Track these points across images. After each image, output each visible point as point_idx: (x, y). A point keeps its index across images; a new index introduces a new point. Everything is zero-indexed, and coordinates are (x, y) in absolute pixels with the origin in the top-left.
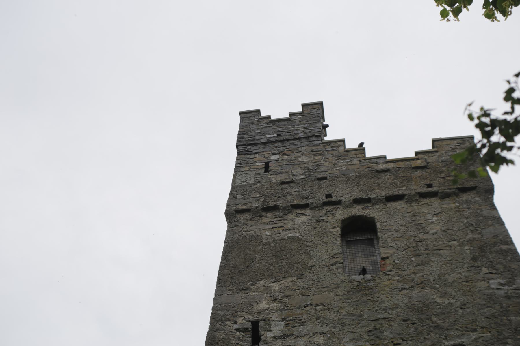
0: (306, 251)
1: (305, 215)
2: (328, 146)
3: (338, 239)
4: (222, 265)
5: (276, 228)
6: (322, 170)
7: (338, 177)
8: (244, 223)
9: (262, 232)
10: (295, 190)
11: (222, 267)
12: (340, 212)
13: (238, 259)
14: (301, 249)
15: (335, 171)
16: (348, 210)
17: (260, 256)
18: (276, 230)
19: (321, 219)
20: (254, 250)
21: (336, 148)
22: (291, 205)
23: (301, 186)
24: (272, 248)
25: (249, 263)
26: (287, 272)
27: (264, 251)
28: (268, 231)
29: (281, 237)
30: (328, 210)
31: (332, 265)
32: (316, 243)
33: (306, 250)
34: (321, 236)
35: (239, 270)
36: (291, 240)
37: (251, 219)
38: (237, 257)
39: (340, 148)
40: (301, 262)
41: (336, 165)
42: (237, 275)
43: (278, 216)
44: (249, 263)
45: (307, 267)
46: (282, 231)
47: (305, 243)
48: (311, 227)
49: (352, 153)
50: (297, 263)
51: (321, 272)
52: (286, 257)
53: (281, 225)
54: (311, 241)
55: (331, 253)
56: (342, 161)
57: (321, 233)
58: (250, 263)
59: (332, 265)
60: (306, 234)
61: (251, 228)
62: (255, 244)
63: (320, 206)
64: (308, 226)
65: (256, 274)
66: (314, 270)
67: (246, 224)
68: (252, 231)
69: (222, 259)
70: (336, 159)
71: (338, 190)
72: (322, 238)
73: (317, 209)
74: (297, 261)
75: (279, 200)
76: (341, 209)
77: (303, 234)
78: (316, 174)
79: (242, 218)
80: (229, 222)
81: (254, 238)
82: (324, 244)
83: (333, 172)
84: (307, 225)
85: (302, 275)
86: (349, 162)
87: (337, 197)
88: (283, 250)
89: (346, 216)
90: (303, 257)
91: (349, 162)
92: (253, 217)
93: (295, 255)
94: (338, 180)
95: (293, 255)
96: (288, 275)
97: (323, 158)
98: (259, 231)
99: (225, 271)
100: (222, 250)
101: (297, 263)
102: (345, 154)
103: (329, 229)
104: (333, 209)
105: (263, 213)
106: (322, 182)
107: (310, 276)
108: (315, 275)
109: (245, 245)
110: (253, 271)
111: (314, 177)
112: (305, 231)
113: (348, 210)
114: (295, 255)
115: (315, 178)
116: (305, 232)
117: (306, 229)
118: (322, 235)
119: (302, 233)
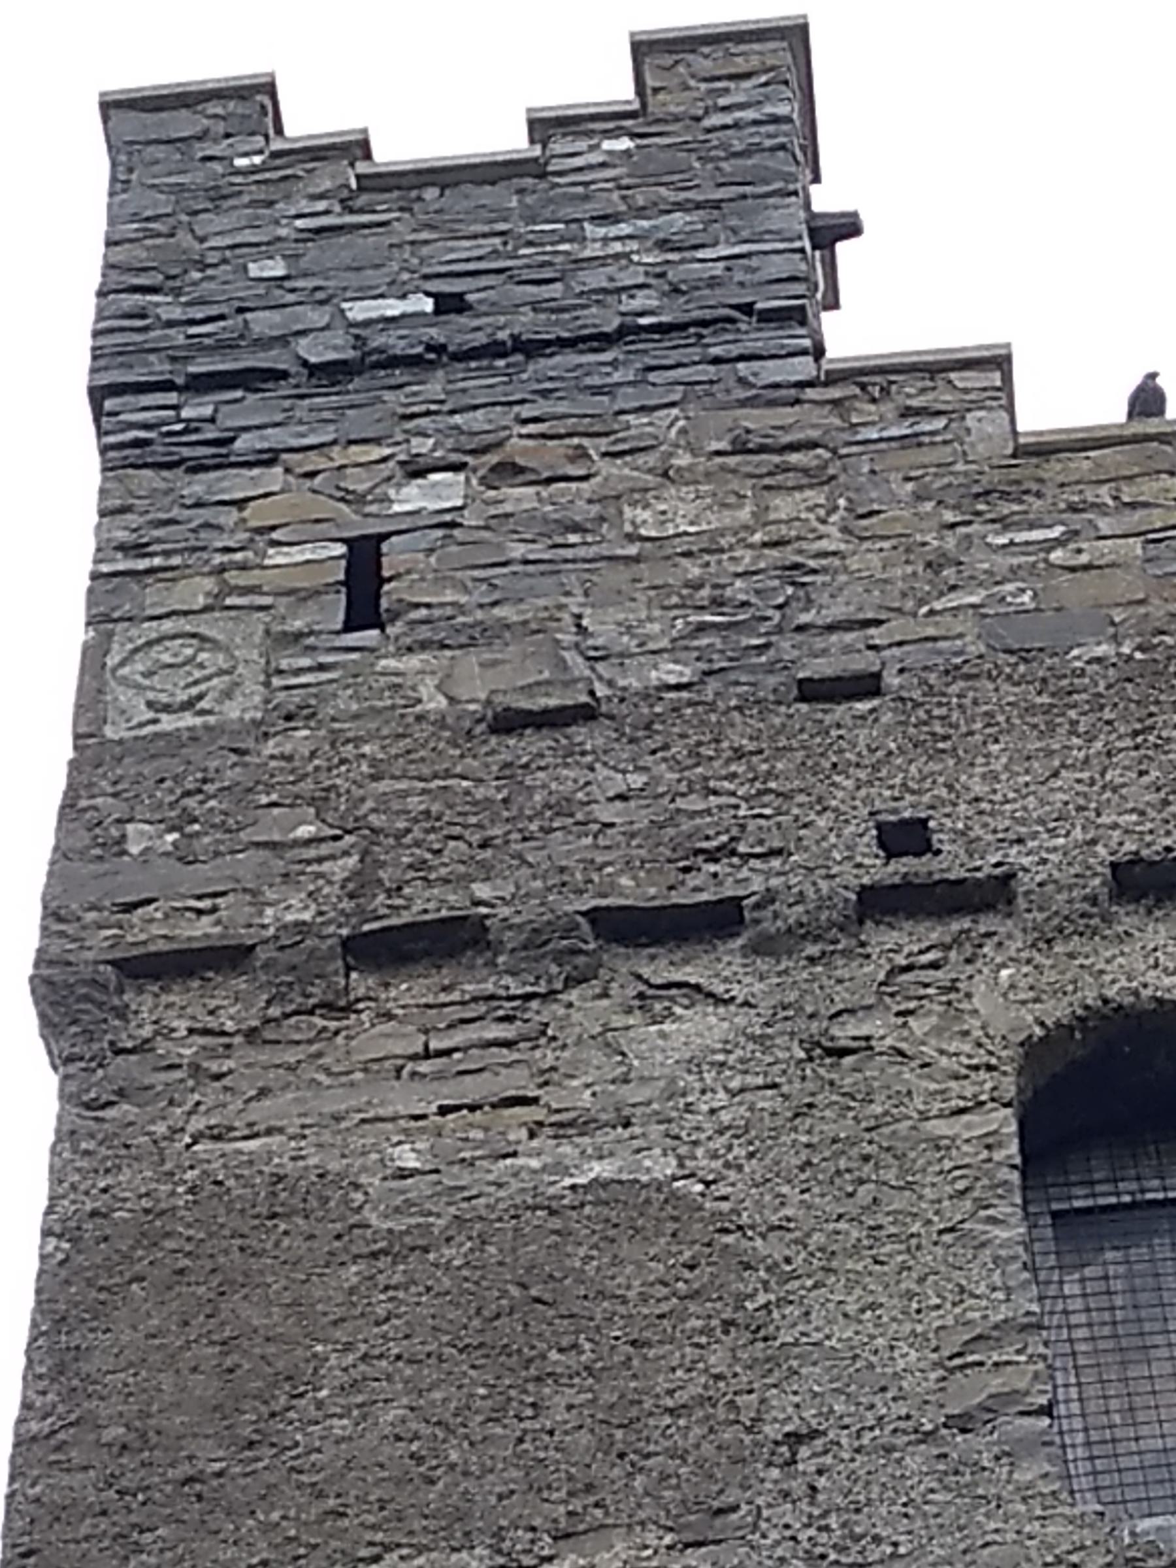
0: (739, 1307)
1: (710, 995)
2: (874, 401)
3: (1002, 1210)
4: (34, 1426)
5: (472, 1108)
6: (837, 611)
7: (968, 677)
8: (195, 1069)
9: (356, 1142)
10: (619, 784)
11: (37, 1450)
12: (1004, 973)
13: (167, 1381)
14: (694, 1295)
15: (948, 618)
16: (1071, 956)
17: (348, 1347)
18: (474, 1127)
19: (845, 1032)
20: (296, 1303)
21: (940, 423)
22: (592, 915)
23: (666, 747)
24: (447, 1282)
25: (264, 1409)
26: (589, 1488)
27: (381, 1311)
28: (405, 1131)
29: (515, 1185)
30: (901, 960)
31: (963, 1424)
32: (817, 1238)
33: (740, 1300)
34: (861, 1182)
35: (185, 1469)
36: (606, 1211)
37: (251, 1035)
38: (155, 1358)
39: (971, 419)
40: (702, 1400)
41: (949, 573)
42: (168, 1520)
43: (482, 1008)
44: (264, 1409)
45: (756, 1444)
46: (523, 1133)
47: (729, 1239)
48: (766, 1101)
49: (1082, 464)
50: (670, 1411)
51: (876, 1490)
52: (571, 1359)
53: (518, 1082)
54: (774, 1219)
55: (949, 1321)
56: (1002, 540)
57: (854, 1152)
58: (273, 1415)
59: (963, 1424)
60: (727, 1165)
61: (260, 1112)
62: (299, 1245)
63: (832, 924)
64: (748, 1096)
65: (332, 1502)
66: (820, 1472)
67: (218, 1077)
68: (269, 1132)
69: (30, 1376)
70: (949, 516)
71: (978, 788)
72: (865, 1193)
73: (813, 950)
74: (670, 1393)
75: (487, 873)
76: (1013, 947)
77: (702, 1162)
78: (786, 646)
79: (182, 1025)
80: (69, 1060)
81: (296, 1202)
82: (888, 1249)
83: (931, 631)
84: (735, 1084)
85: (720, 1512)
86: (1059, 543)
87: (972, 846)
88: (547, 1297)
89: (1057, 1011)
90: (717, 1359)
91: (1059, 543)
92: (275, 1011)
93: (648, 1344)
94: (975, 702)
95: (633, 1343)
96: (598, 1513)
97: (835, 508)
98: (326, 1137)
99: (66, 1480)
100: (29, 1300)
101: (670, 1411)
102: (1015, 474)
103: (924, 1117)
104: (947, 948)
105: (361, 983)
106: (840, 711)
107: (788, 1519)
108: (825, 1514)
109: (222, 1260)
110: (304, 1478)
111: (770, 668)
112: (721, 1132)
113: (1071, 956)
114: (648, 1344)
115: (781, 678)
116: (719, 1143)
117: (725, 1117)
118: (867, 1168)
119: (700, 1152)
